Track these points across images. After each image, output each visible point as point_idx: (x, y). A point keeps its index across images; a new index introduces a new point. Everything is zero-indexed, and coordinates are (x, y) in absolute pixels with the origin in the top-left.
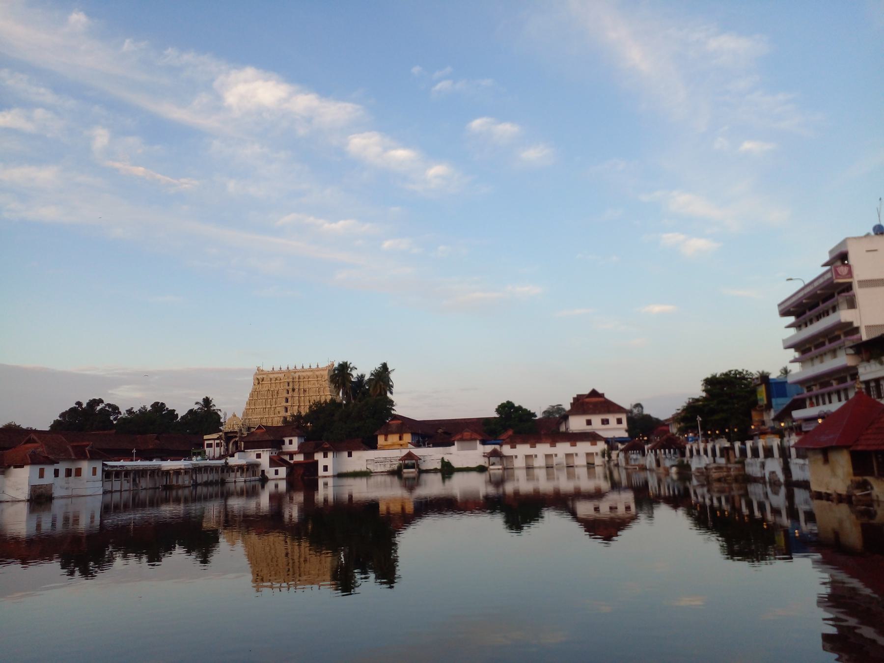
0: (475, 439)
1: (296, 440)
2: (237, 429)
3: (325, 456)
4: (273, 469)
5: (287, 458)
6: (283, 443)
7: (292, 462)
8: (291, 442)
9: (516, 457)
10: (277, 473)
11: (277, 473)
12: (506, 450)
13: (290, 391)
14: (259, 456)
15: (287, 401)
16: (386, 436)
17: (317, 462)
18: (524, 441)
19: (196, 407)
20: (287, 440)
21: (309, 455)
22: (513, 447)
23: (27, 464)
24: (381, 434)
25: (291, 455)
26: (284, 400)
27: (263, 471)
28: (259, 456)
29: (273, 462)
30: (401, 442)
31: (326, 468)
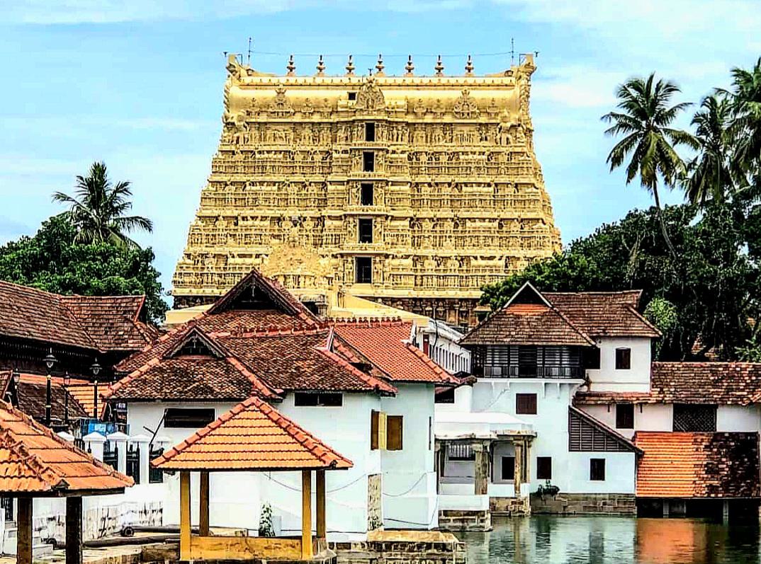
1: (641, 354)
4: (583, 459)
5: (607, 418)
7: (626, 434)
8: (623, 360)
10: (598, 470)
11: (598, 470)
13: (379, 159)
14: (527, 404)
15: (367, 197)
19: (67, 207)
20: (608, 351)
26: (356, 192)
27: (545, 467)
28: (527, 404)
29: (584, 433)
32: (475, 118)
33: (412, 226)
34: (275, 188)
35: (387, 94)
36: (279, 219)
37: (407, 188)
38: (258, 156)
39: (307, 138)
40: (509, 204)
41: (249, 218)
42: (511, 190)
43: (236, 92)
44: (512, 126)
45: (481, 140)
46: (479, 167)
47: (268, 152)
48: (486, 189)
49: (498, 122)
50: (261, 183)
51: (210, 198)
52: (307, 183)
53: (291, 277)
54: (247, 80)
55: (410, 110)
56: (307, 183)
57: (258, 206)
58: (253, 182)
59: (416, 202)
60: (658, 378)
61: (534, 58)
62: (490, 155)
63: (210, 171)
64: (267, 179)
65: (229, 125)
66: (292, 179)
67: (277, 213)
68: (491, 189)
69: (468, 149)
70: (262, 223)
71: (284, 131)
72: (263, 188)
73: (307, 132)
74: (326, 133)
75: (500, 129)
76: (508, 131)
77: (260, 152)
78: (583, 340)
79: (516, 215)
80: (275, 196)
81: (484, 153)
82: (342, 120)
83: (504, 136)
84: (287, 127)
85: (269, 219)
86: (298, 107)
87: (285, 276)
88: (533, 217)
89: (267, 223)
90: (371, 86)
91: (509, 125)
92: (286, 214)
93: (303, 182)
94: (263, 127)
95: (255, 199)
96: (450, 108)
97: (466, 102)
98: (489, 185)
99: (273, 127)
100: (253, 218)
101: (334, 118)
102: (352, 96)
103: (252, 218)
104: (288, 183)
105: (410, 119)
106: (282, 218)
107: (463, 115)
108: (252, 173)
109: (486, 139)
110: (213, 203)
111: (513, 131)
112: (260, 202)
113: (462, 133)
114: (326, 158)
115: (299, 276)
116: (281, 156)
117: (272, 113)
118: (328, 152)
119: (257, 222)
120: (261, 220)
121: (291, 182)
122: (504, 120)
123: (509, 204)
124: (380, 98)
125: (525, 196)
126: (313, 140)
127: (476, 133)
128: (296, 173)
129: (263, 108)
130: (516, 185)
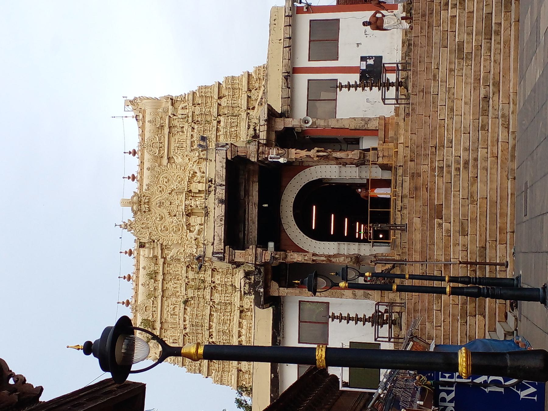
2: (216, 169)
32: (164, 137)
34: (215, 314)
36: (241, 312)
38: (187, 330)
39: (175, 285)
40: (235, 102)
41: (239, 339)
42: (224, 102)
44: (172, 104)
45: (183, 132)
46: (204, 131)
47: (184, 321)
48: (222, 124)
49: (168, 117)
50: (210, 327)
51: (222, 376)
52: (213, 285)
53: (187, 202)
56: (213, 285)
57: (229, 331)
58: (210, 336)
61: (127, 99)
62: (195, 123)
63: (198, 375)
64: (207, 321)
66: (208, 297)
67: (237, 313)
68: (222, 118)
69: (189, 142)
70: (244, 327)
71: (168, 306)
72: (214, 325)
73: (170, 286)
74: (171, 269)
75: (174, 115)
76: (176, 109)
77: (185, 328)
79: (245, 97)
80: (222, 315)
81: (193, 128)
82: (160, 252)
83: (180, 111)
84: (166, 303)
85: (241, 320)
87: (189, 215)
88: (247, 79)
89: (244, 322)
90: (130, 225)
91: (170, 107)
92: (238, 304)
93: (212, 288)
94: (165, 326)
95: (224, 333)
98: (219, 122)
99: (165, 316)
100: (240, 336)
103: (240, 336)
104: (211, 303)
106: (241, 309)
107: (161, 147)
108: (202, 337)
109: (183, 127)
110: (226, 373)
111: (176, 105)
112: (226, 328)
113: (176, 148)
114: (192, 268)
115: (190, 191)
116: (189, 309)
117: (153, 316)
118: (188, 267)
119: (243, 332)
120: (242, 328)
121: (211, 300)
122: (166, 111)
123: (235, 102)
125: (229, 88)
126: (178, 280)
127: (176, 137)
128: (203, 295)
130: (220, 98)
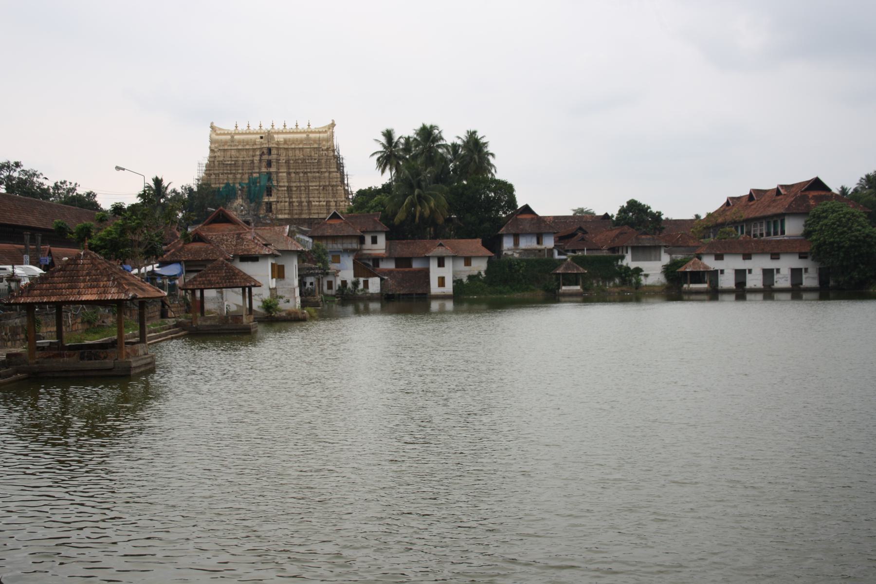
0: (660, 247)
1: (382, 240)
3: (441, 264)
6: (362, 240)
8: (374, 241)
9: (722, 272)
12: (710, 262)
13: (274, 164)
16: (516, 237)
17: (426, 273)
18: (733, 253)
21: (403, 262)
22: (719, 257)
23: (266, 256)
24: (508, 235)
25: (376, 260)
30: (539, 247)
31: (442, 282)
33: (288, 190)
35: (275, 136)
37: (285, 174)
43: (215, 137)
54: (219, 132)
55: (285, 142)
59: (289, 181)
60: (388, 248)
65: (212, 151)
78: (358, 233)
86: (239, 142)
96: (301, 141)
97: (308, 139)
101: (255, 147)
102: (262, 138)
105: (286, 146)
124: (273, 138)
129: (225, 143)
